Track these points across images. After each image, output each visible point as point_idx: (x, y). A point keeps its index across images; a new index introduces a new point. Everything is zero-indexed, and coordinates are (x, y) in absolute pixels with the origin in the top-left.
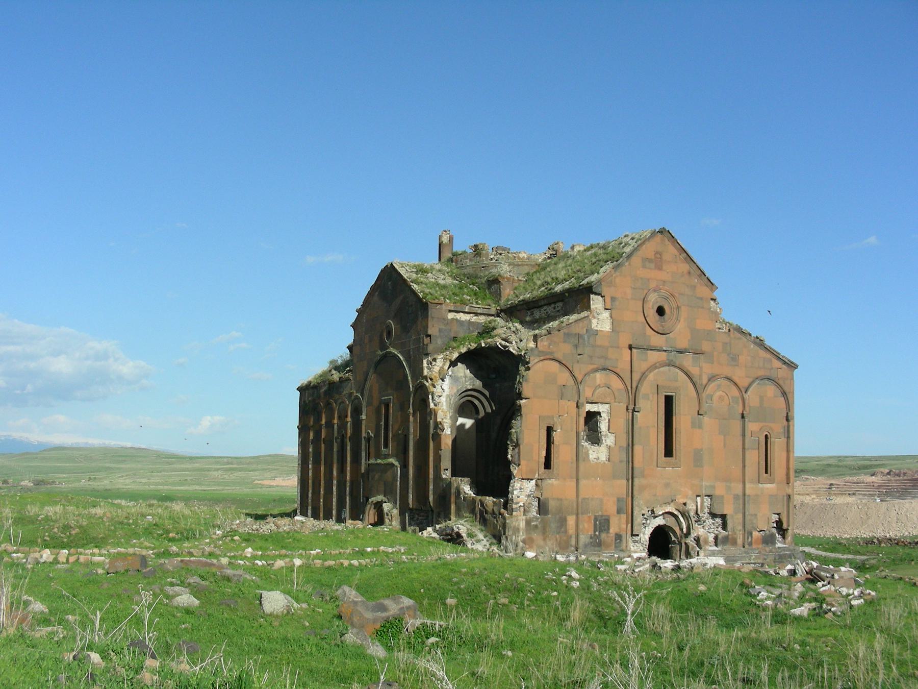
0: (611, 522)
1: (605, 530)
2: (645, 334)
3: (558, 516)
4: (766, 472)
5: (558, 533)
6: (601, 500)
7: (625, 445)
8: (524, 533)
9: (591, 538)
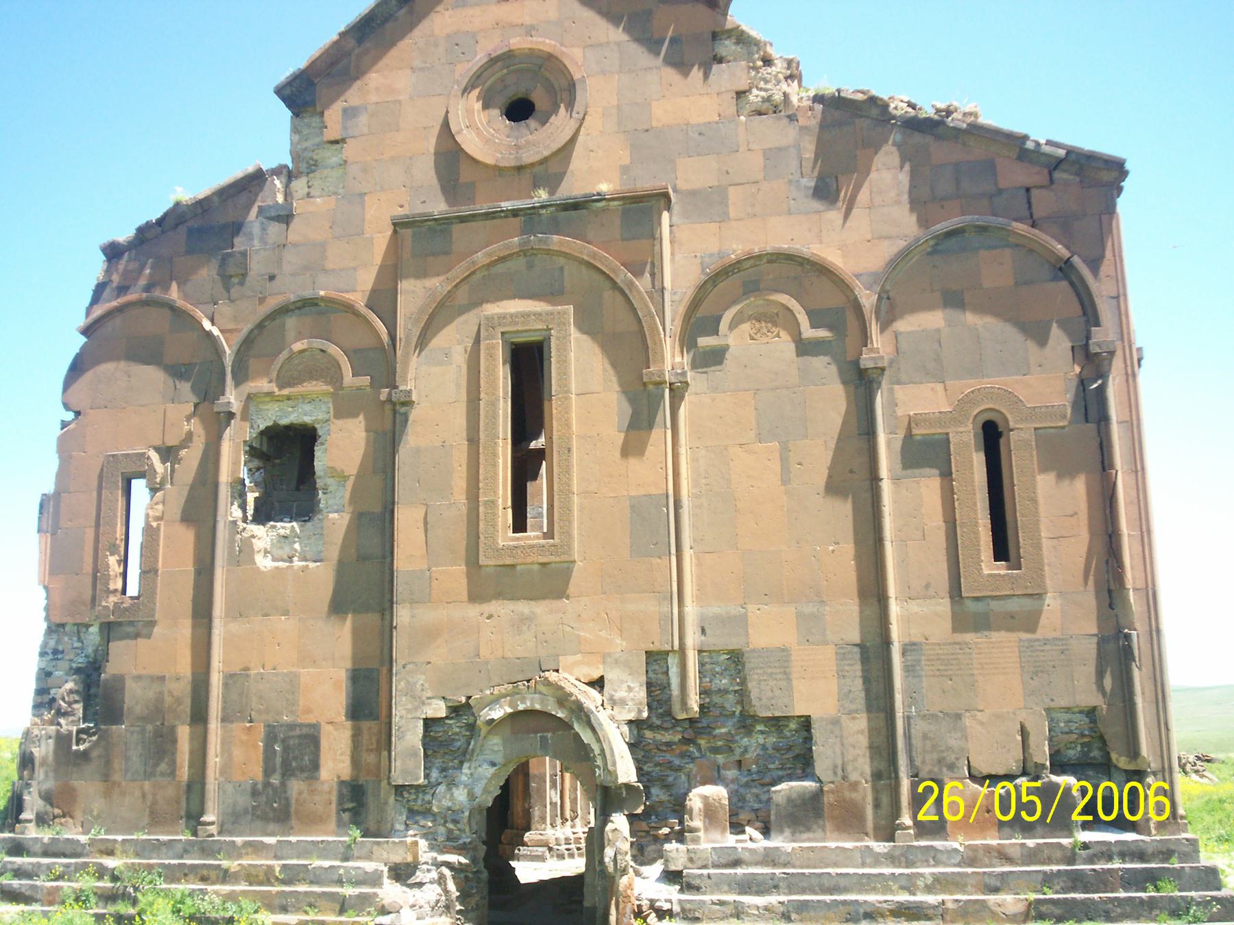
0: (324, 744)
1: (302, 770)
2: (458, 180)
3: (150, 728)
4: (1002, 550)
5: (148, 775)
6: (293, 679)
7: (378, 509)
8: (51, 774)
9: (255, 793)
